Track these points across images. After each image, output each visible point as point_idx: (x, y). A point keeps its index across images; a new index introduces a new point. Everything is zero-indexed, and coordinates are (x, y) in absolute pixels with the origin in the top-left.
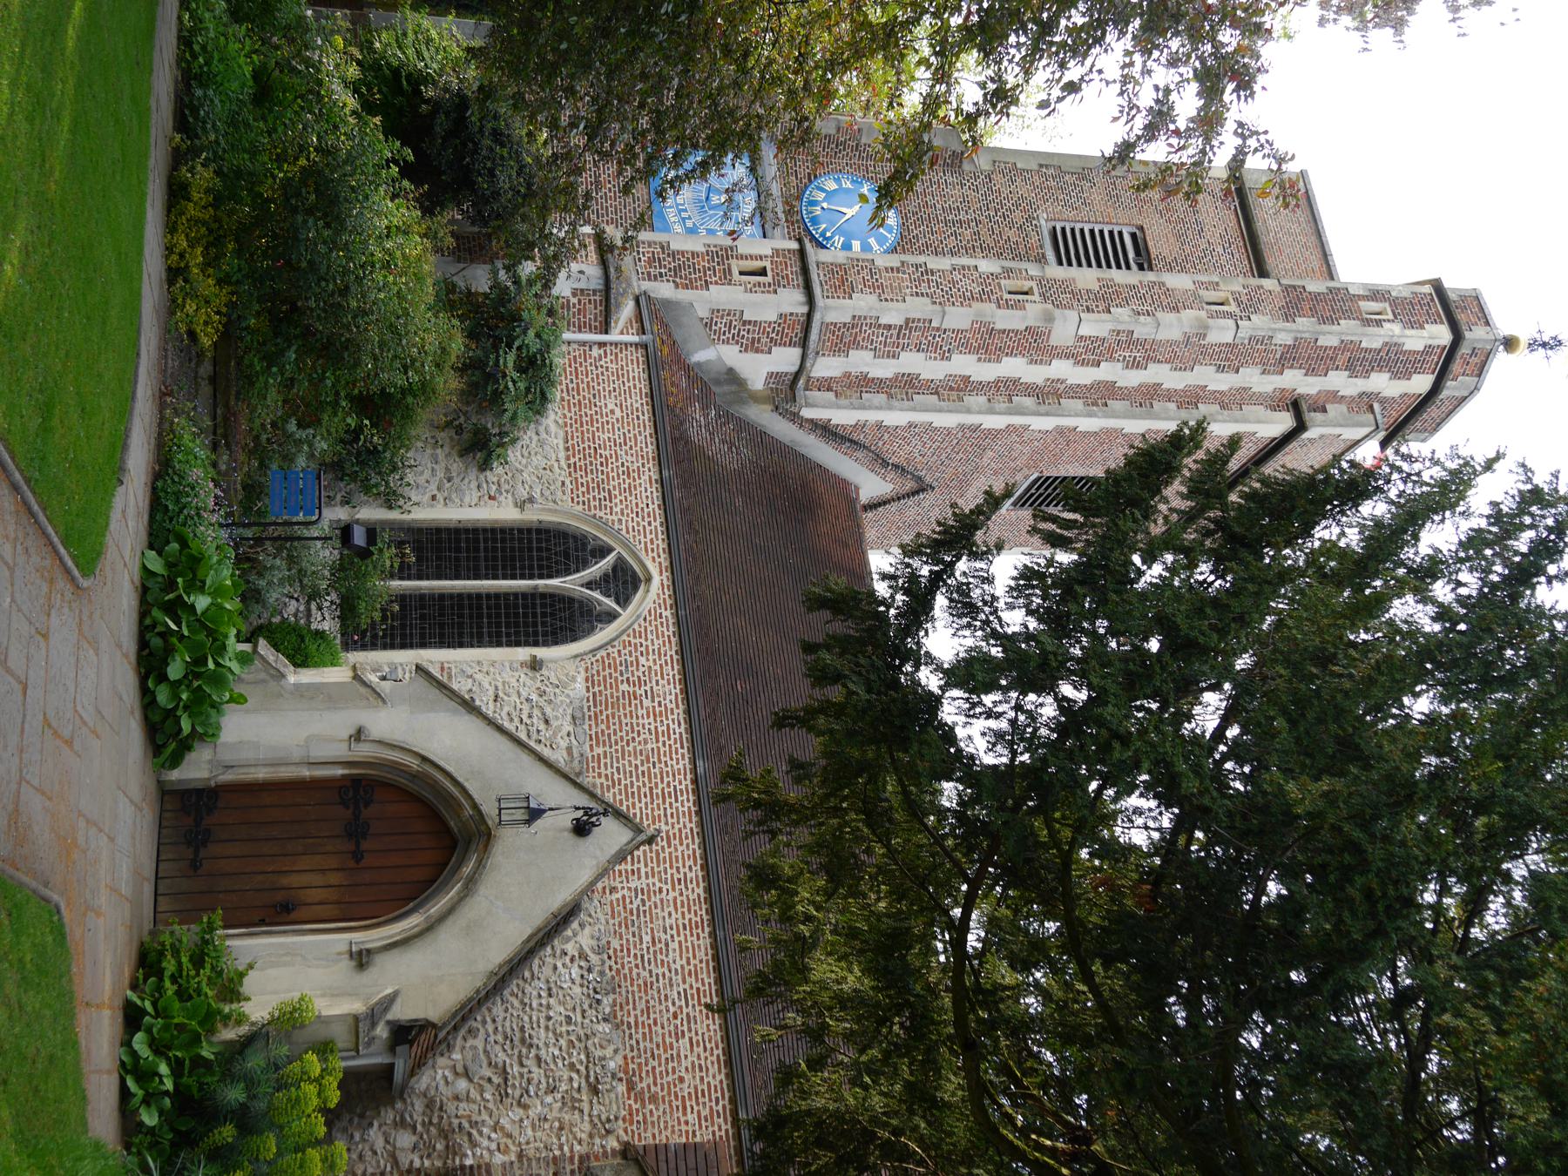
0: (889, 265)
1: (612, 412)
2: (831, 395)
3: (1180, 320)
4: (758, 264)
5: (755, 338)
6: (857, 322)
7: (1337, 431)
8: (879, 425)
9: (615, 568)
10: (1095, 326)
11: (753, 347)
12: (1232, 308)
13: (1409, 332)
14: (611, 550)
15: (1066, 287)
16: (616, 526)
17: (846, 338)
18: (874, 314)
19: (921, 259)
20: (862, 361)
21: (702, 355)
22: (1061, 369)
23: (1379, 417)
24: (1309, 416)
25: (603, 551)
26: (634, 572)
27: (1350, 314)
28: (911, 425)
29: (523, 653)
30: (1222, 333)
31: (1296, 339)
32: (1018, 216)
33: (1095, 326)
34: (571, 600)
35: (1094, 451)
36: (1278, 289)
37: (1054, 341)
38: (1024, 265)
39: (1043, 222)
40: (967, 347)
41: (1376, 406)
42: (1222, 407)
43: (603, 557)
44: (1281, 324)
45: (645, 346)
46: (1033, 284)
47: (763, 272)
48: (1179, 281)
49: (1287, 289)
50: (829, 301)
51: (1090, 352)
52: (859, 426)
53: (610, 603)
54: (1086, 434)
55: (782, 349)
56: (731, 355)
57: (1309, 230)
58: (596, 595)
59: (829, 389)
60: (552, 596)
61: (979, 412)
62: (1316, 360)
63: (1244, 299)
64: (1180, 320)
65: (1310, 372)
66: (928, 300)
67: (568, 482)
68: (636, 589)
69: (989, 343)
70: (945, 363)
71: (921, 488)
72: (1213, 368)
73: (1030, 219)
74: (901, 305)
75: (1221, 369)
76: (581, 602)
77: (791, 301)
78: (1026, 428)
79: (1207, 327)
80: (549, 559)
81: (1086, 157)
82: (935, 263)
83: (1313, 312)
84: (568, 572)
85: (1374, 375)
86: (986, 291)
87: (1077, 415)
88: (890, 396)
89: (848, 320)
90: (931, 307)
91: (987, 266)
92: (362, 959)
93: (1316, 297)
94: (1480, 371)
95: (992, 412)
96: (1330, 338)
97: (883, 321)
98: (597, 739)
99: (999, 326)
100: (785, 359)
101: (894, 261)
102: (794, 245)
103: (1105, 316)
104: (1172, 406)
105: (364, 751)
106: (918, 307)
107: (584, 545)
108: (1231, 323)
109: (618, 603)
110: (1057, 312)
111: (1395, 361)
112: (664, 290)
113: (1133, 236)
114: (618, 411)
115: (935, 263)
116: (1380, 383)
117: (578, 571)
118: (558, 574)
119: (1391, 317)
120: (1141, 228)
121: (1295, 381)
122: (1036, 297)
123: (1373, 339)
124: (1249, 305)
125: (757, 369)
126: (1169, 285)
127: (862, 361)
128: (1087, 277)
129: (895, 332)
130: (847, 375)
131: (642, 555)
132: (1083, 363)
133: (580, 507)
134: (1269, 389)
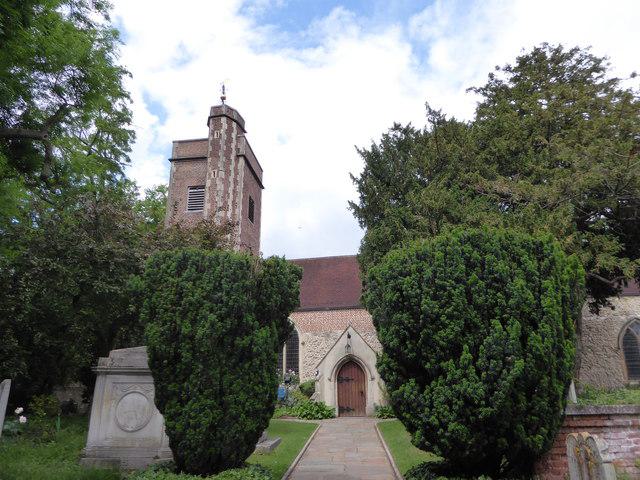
29: (300, 346)
30: (222, 174)
62: (228, 152)
81: (307, 260)
92: (373, 379)
93: (214, 148)
94: (230, 110)
98: (320, 330)
105: (333, 378)
116: (234, 135)
121: (233, 157)
123: (225, 137)
124: (215, 167)
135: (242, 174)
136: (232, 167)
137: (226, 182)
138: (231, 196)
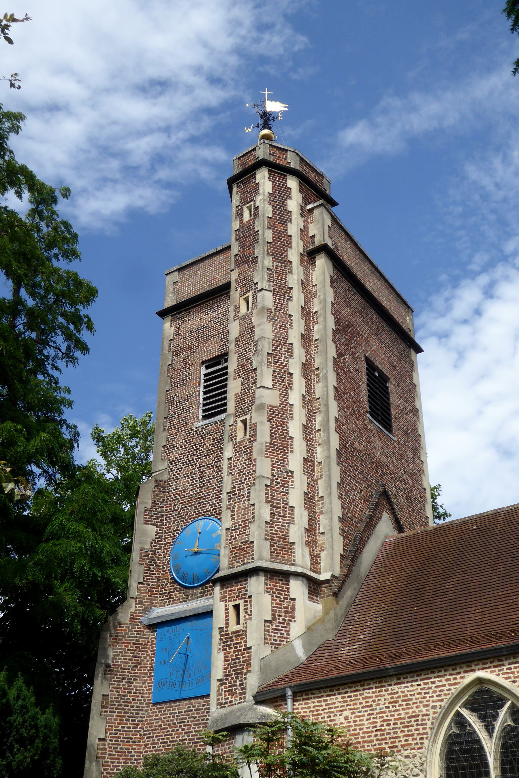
0: (229, 518)
1: (346, 718)
2: (323, 555)
3: (259, 325)
4: (232, 612)
5: (284, 612)
6: (271, 538)
7: (326, 228)
8: (341, 520)
9: (473, 710)
10: (266, 377)
11: (290, 612)
12: (250, 294)
13: (261, 191)
14: (458, 713)
15: (240, 398)
16: (438, 710)
17: (282, 545)
18: (263, 525)
19: (225, 496)
20: (296, 533)
21: (300, 652)
22: (295, 398)
23: (316, 204)
24: (318, 241)
25: (460, 720)
26: (475, 694)
27: (251, 225)
28: (340, 497)
30: (267, 299)
31: (268, 255)
32: (197, 441)
33: (266, 377)
34: (504, 746)
35: (350, 377)
36: (237, 270)
37: (277, 403)
38: (227, 428)
39: (200, 424)
40: (283, 461)
41: (309, 207)
42: (315, 296)
43: (465, 720)
44: (260, 264)
45: (295, 694)
46: (239, 420)
47: (237, 607)
48: (234, 329)
49: (237, 265)
50: (255, 557)
51: (282, 379)
52: (344, 534)
53: (503, 712)
54: (339, 382)
55: (291, 590)
56: (297, 629)
57: (201, 265)
58: (498, 725)
59: (318, 556)
60: (503, 763)
61: (329, 449)
62: (282, 241)
63: (244, 289)
64: (259, 325)
65: (289, 245)
66: (252, 488)
67: (406, 753)
68: (489, 692)
69: (280, 446)
70: (295, 474)
71: (385, 495)
72: (290, 303)
73: (198, 433)
74: (256, 507)
75: (290, 298)
76: (505, 738)
77: (256, 585)
78: (337, 420)
79: (263, 308)
80: (471, 767)
82: (227, 486)
83: (251, 247)
84: (482, 750)
85: (289, 209)
86: (245, 450)
87: (327, 386)
88: (321, 513)
89: (268, 544)
90: (257, 486)
91: (228, 452)
95: (327, 442)
96: (269, 236)
97: (268, 519)
99: (268, 439)
100: (297, 589)
101: (226, 516)
102: (217, 589)
103: (258, 371)
104: (316, 327)
106: (258, 495)
107: (456, 736)
108: (259, 294)
109: (502, 706)
110: (257, 402)
111: (279, 198)
112: (253, 682)
113: (207, 368)
114: (345, 714)
115: (227, 486)
116: (293, 204)
117: (479, 742)
118: (484, 758)
119: (252, 203)
120: (203, 363)
122: (248, 417)
123: (267, 210)
125: (306, 609)
126: (237, 335)
127: (296, 533)
128: (234, 386)
129: (276, 510)
130: (308, 543)
131: (459, 687)
132: (290, 383)
133: (426, 741)
134: (302, 269)
135: (325, 294)
136: (294, 280)
137: (279, 316)
138: (298, 351)
